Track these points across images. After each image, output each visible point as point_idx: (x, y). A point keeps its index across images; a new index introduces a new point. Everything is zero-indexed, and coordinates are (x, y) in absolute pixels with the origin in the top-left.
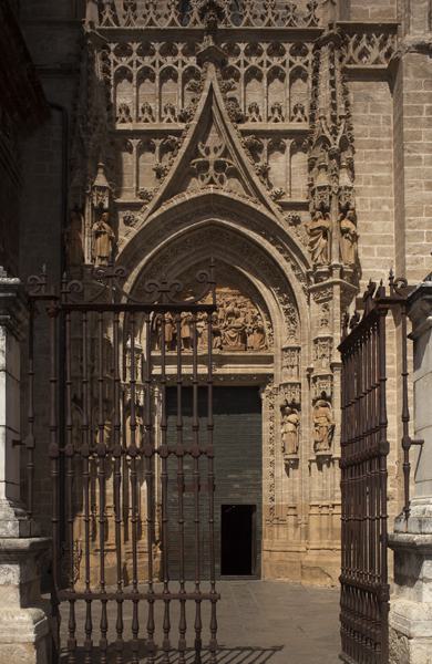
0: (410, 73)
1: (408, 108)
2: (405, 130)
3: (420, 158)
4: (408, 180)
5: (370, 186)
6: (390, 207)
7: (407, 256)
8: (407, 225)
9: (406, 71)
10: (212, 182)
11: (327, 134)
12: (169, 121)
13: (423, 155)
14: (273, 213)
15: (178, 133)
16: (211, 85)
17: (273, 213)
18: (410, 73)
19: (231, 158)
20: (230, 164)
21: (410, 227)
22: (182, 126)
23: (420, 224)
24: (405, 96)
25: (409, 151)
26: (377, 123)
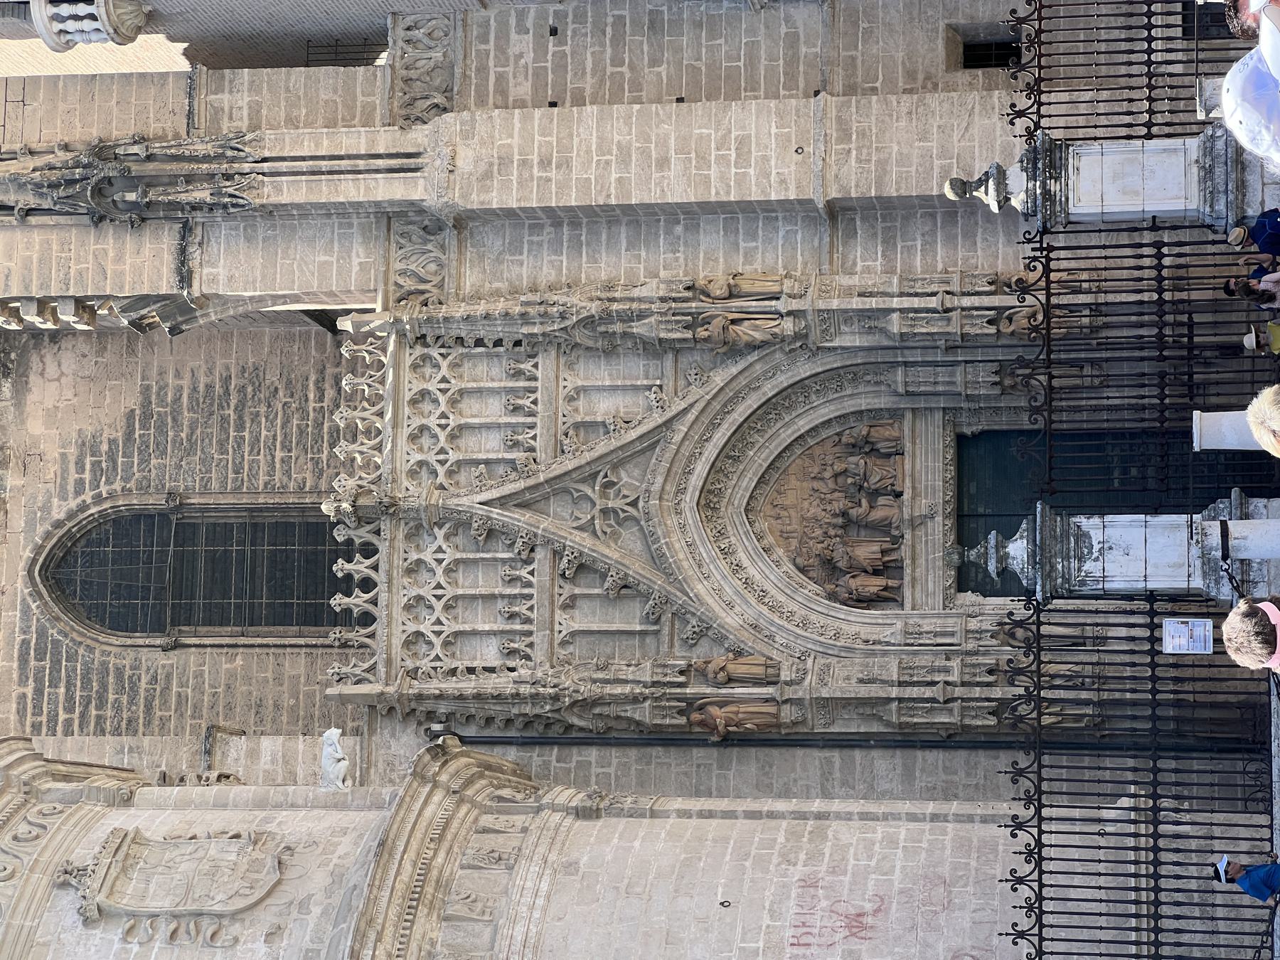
1: (539, 200)
2: (573, 204)
3: (619, 180)
4: (653, 197)
7: (773, 197)
8: (725, 199)
13: (614, 176)
14: (692, 405)
17: (692, 405)
20: (606, 476)
21: (728, 193)
23: (723, 178)
24: (522, 205)
25: (609, 196)
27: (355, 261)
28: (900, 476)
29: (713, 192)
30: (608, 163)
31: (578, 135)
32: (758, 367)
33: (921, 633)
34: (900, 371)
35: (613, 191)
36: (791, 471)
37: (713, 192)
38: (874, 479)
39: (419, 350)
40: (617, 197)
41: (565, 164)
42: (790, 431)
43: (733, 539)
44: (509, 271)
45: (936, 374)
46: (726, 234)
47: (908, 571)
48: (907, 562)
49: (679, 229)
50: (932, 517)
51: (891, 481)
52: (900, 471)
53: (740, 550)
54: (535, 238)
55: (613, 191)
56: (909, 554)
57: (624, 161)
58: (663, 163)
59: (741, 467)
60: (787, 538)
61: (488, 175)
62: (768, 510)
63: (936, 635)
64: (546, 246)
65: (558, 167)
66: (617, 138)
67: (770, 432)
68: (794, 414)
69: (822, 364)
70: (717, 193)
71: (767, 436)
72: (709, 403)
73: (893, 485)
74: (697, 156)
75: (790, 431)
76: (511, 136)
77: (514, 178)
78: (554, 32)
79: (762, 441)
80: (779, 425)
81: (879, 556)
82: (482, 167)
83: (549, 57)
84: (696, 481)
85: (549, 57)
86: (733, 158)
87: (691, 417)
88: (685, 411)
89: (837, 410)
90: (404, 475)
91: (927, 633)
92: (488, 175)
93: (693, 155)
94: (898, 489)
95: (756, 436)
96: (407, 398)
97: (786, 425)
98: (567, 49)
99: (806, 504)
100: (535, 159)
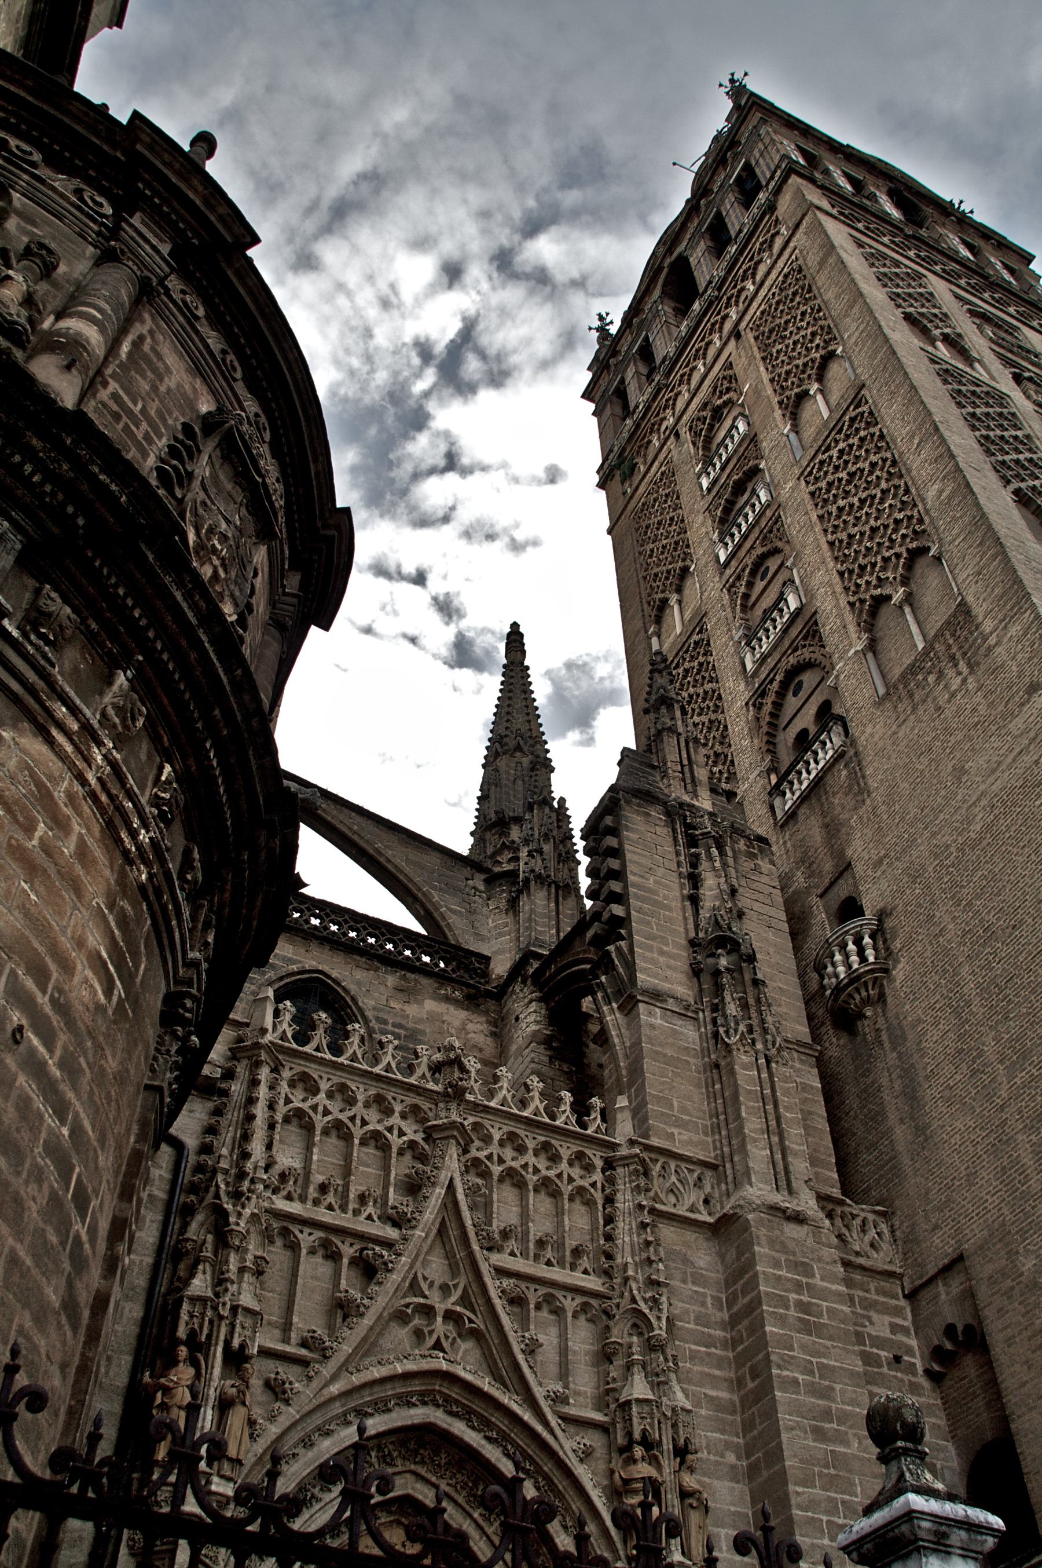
0: (763, 1240)
1: (767, 1293)
3: (796, 1381)
5: (703, 1412)
6: (739, 1458)
9: (758, 1237)
10: (438, 1346)
11: (644, 1307)
12: (369, 1218)
14: (552, 1432)
15: (388, 1244)
16: (451, 1180)
18: (763, 1240)
19: (474, 1312)
20: (471, 1321)
21: (800, 1507)
22: (391, 1233)
24: (761, 1276)
26: (703, 1304)
27: (676, 1131)
29: (800, 1489)
30: (811, 1373)
31: (834, 1347)
35: (785, 1373)
37: (800, 1489)
39: (599, 1163)
40: (779, 1376)
41: (807, 1328)
44: (676, 1268)
46: (734, 1514)
49: (731, 1458)
54: (709, 1300)
55: (785, 1373)
57: (814, 1390)
58: (820, 1434)
61: (785, 1249)
64: (702, 1309)
65: (800, 1319)
66: (838, 1387)
70: (797, 1493)
72: (552, 1454)
74: (832, 1476)
76: (822, 1279)
77: (782, 1273)
78: (897, 1359)
82: (791, 1245)
83: (875, 1350)
84: (459, 1428)
85: (875, 1350)
86: (836, 1519)
87: (539, 1428)
88: (546, 1424)
90: (479, 1120)
92: (785, 1249)
93: (832, 1471)
96: (553, 1142)
98: (885, 1370)
100: (805, 1298)
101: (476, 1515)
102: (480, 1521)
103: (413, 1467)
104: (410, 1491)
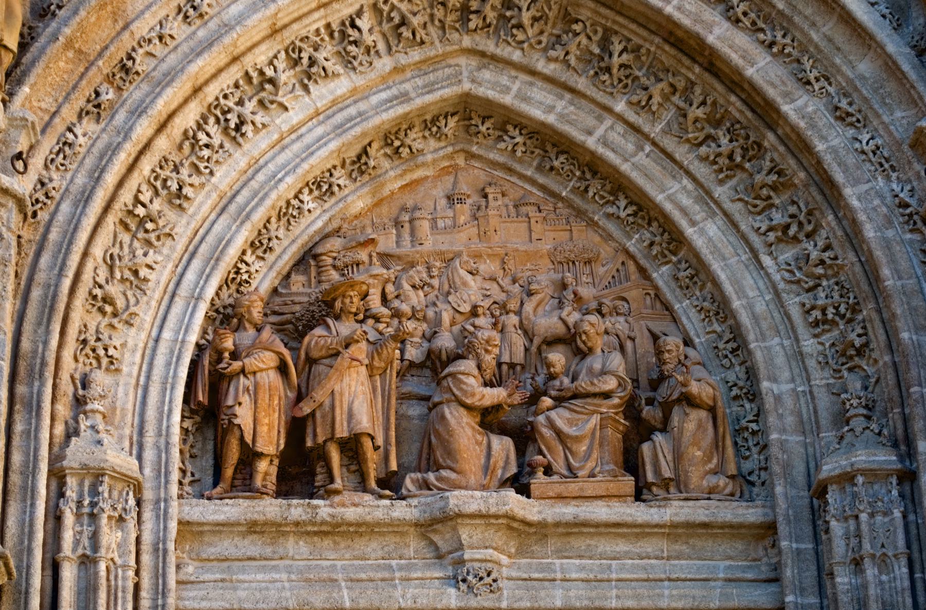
28: (573, 487)
32: (865, 67)
33: (93, 517)
34: (886, 458)
36: (578, 227)
38: (560, 417)
42: (686, 201)
43: (384, 64)
45: (883, 562)
47: (297, 509)
48: (323, 509)
50: (456, 580)
51: (559, 466)
52: (590, 488)
53: (359, 81)
56: (351, 513)
59: (581, 83)
60: (398, 224)
62: (477, 174)
63: (87, 562)
67: (681, 152)
68: (735, 209)
69: (887, 245)
71: (669, 144)
73: (548, 471)
75: (686, 201)
79: (655, 130)
80: (702, 171)
81: (342, 432)
89: (755, 318)
91: (95, 538)
94: (539, 480)
95: (669, 114)
97: (705, 194)
99: (489, 267)
101: (620, 107)
102: (632, 117)
103: (467, 42)
104: (467, 86)
